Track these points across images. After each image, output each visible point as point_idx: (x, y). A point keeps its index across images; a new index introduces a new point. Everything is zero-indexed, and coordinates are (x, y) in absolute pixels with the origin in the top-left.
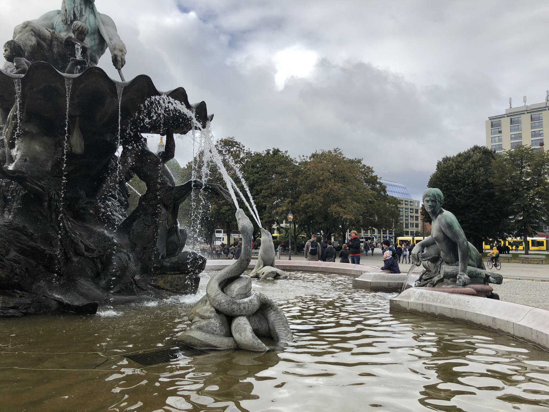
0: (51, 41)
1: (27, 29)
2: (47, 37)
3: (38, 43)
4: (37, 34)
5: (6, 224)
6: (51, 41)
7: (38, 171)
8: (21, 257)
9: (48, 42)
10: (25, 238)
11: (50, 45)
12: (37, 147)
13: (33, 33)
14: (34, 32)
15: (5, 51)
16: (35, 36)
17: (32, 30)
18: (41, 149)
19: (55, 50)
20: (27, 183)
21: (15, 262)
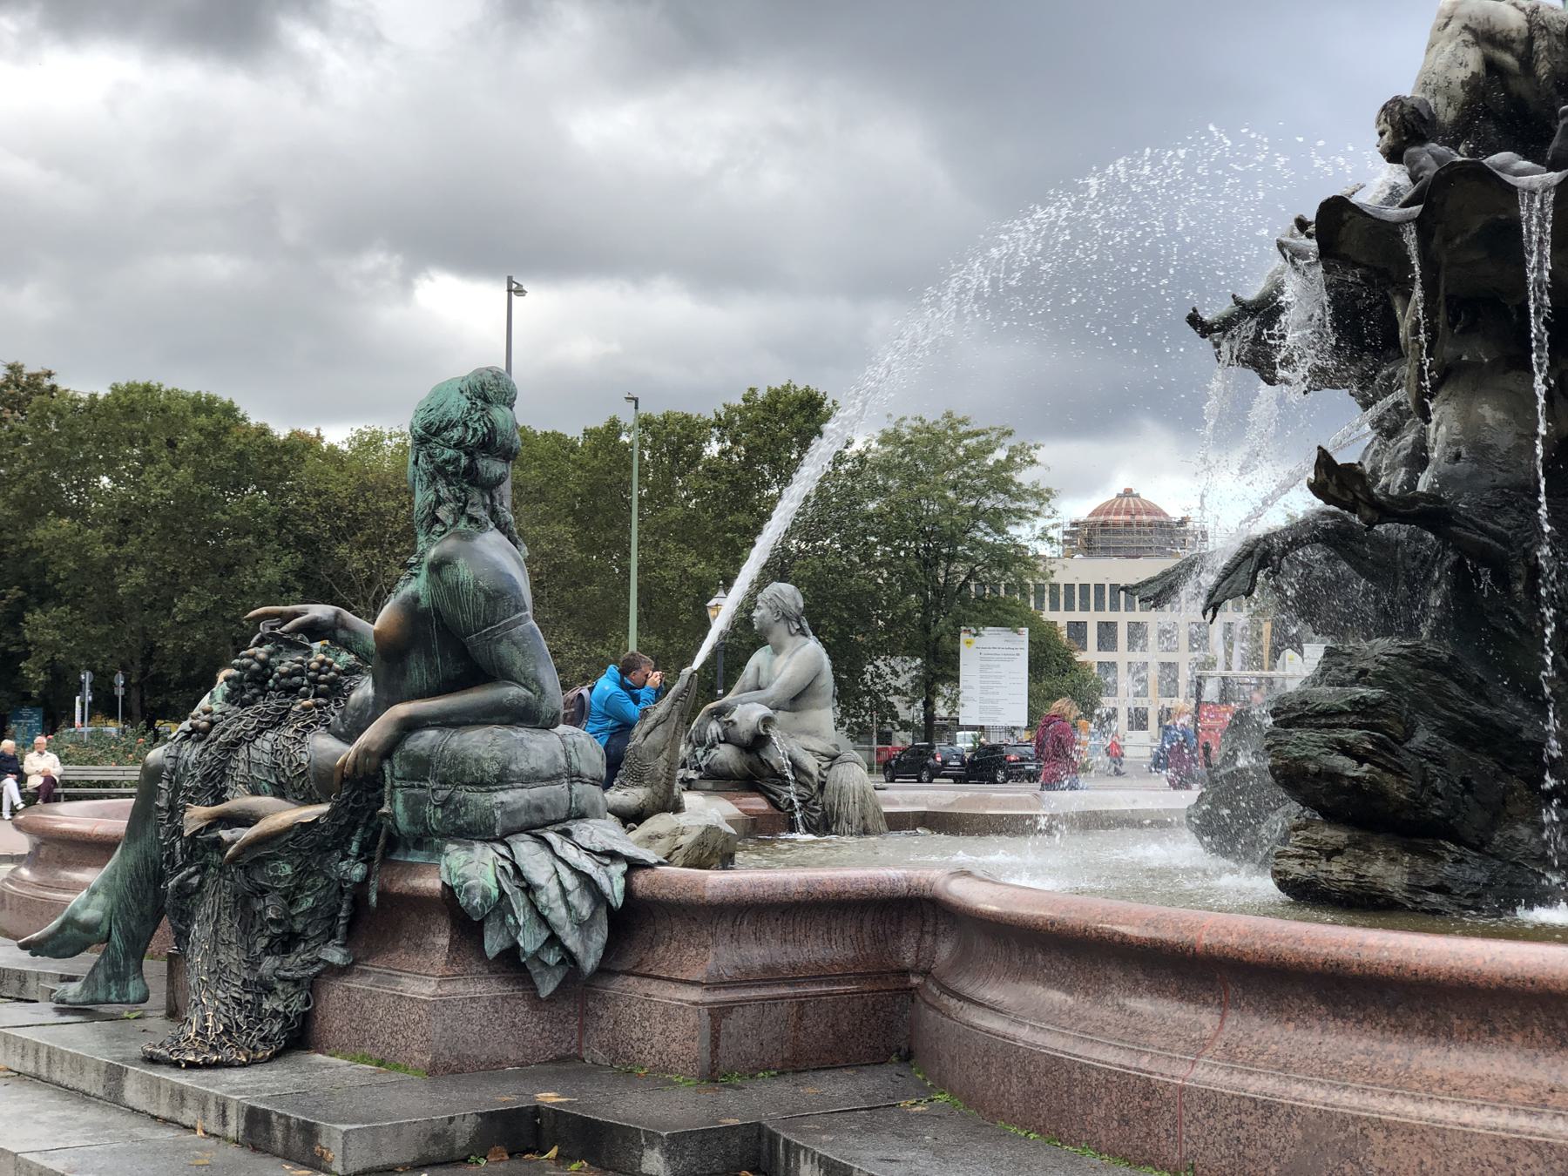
0: (1530, 40)
1: (1449, 28)
2: (1514, 34)
3: (1490, 65)
4: (1485, 36)
5: (1405, 651)
6: (1530, 40)
7: (1494, 488)
8: (1447, 746)
9: (1520, 48)
10: (1455, 690)
11: (1527, 60)
12: (1488, 412)
13: (1468, 37)
14: (1473, 32)
15: (1382, 134)
16: (1477, 43)
17: (1466, 27)
18: (1500, 415)
19: (1543, 69)
20: (1454, 529)
21: (1430, 760)
